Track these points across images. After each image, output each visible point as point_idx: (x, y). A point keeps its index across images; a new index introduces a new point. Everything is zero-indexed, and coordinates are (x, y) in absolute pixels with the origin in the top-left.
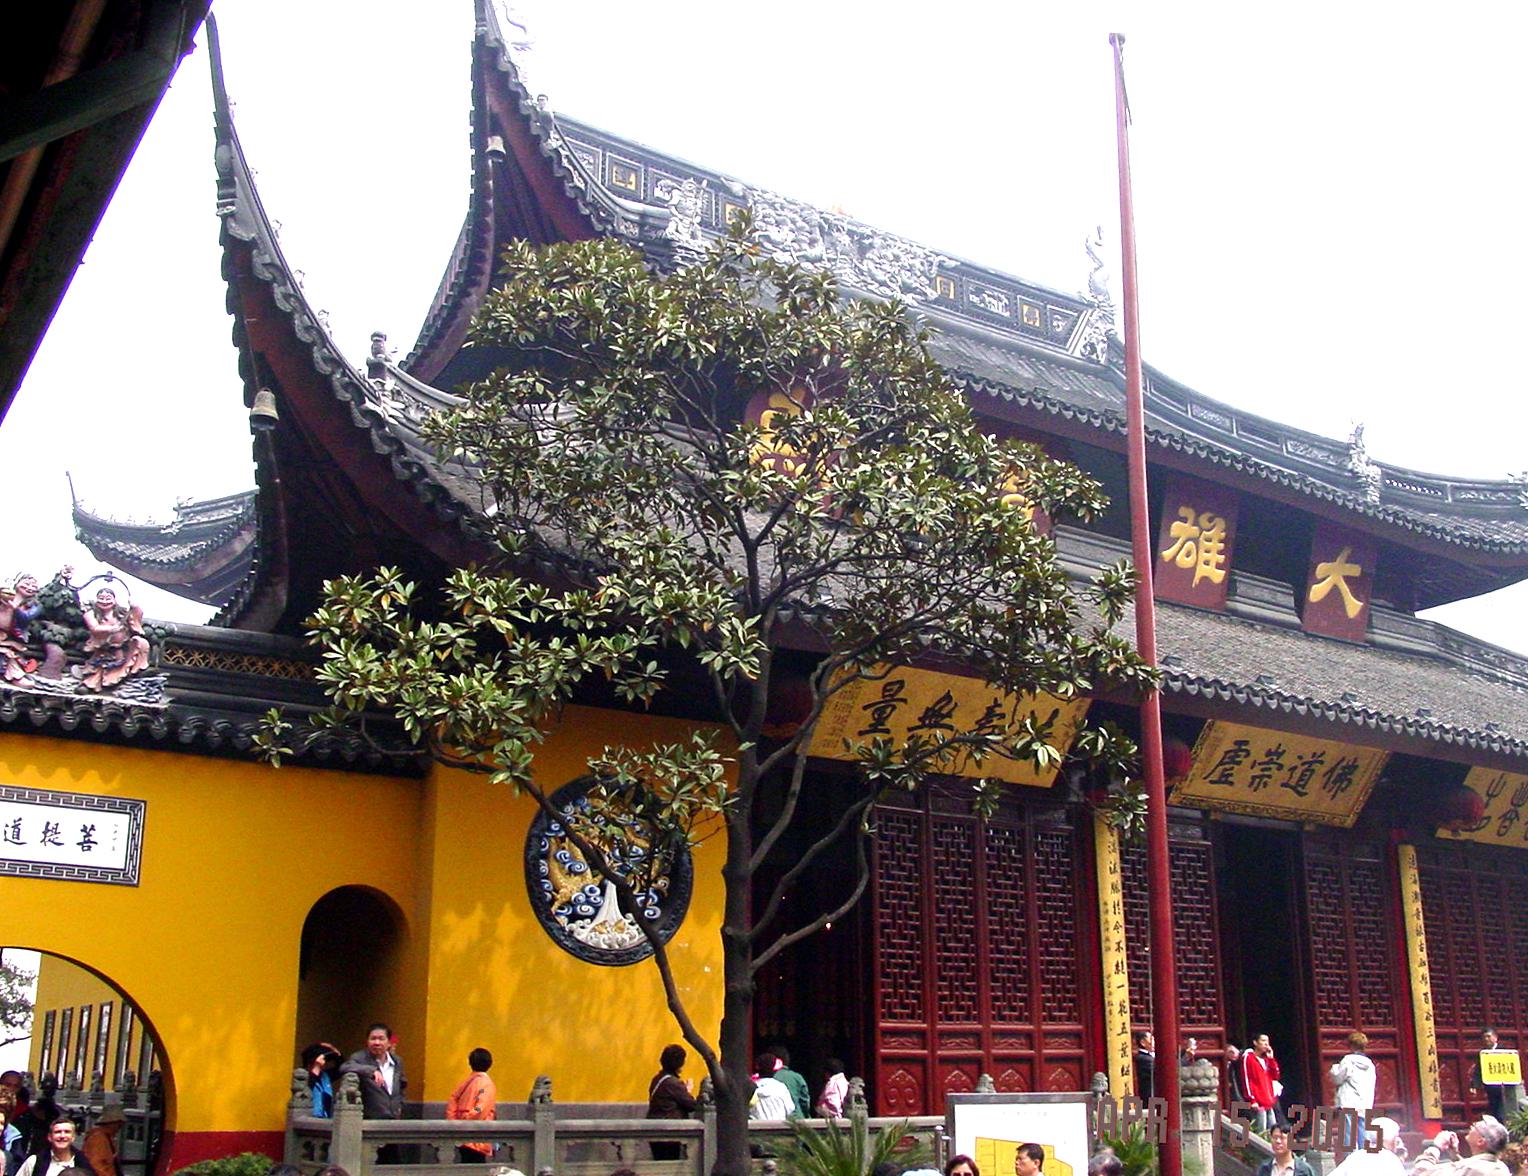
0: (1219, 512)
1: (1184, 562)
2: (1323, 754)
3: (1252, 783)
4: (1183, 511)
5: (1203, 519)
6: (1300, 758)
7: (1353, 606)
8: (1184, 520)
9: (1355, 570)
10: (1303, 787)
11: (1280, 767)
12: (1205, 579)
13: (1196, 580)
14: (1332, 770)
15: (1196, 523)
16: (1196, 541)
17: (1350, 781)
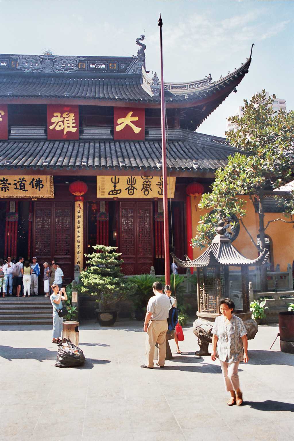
0: (70, 112)
1: (58, 128)
2: (24, 178)
3: (2, 190)
4: (55, 114)
5: (65, 115)
6: (15, 181)
7: (137, 130)
8: (57, 116)
9: (136, 119)
10: (24, 188)
11: (10, 184)
12: (69, 132)
13: (65, 132)
14: (32, 182)
15: (62, 116)
16: (63, 122)
17: (43, 185)
